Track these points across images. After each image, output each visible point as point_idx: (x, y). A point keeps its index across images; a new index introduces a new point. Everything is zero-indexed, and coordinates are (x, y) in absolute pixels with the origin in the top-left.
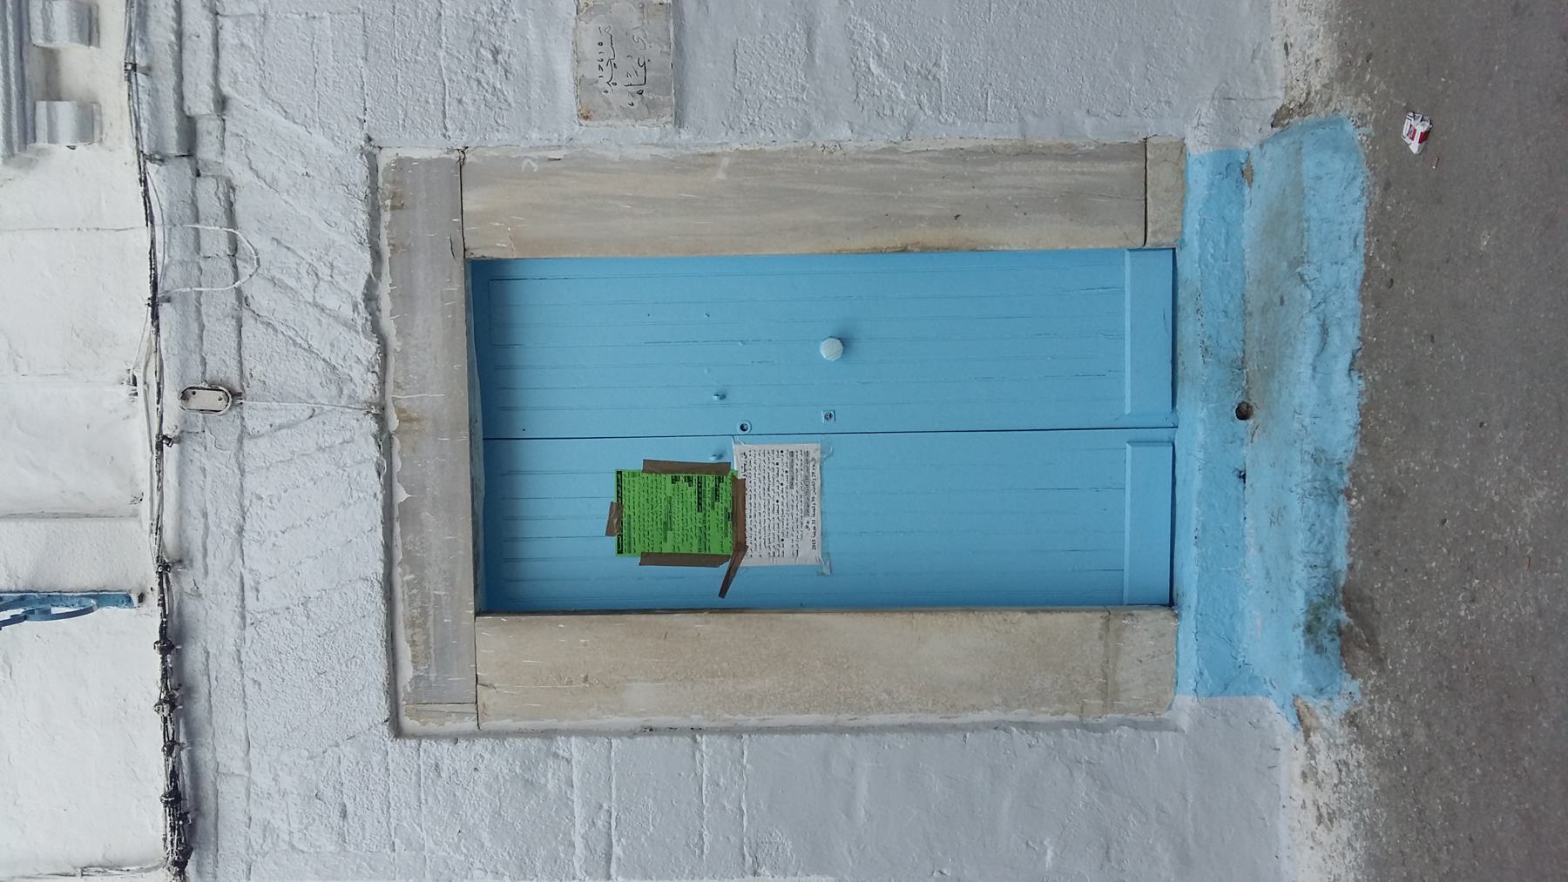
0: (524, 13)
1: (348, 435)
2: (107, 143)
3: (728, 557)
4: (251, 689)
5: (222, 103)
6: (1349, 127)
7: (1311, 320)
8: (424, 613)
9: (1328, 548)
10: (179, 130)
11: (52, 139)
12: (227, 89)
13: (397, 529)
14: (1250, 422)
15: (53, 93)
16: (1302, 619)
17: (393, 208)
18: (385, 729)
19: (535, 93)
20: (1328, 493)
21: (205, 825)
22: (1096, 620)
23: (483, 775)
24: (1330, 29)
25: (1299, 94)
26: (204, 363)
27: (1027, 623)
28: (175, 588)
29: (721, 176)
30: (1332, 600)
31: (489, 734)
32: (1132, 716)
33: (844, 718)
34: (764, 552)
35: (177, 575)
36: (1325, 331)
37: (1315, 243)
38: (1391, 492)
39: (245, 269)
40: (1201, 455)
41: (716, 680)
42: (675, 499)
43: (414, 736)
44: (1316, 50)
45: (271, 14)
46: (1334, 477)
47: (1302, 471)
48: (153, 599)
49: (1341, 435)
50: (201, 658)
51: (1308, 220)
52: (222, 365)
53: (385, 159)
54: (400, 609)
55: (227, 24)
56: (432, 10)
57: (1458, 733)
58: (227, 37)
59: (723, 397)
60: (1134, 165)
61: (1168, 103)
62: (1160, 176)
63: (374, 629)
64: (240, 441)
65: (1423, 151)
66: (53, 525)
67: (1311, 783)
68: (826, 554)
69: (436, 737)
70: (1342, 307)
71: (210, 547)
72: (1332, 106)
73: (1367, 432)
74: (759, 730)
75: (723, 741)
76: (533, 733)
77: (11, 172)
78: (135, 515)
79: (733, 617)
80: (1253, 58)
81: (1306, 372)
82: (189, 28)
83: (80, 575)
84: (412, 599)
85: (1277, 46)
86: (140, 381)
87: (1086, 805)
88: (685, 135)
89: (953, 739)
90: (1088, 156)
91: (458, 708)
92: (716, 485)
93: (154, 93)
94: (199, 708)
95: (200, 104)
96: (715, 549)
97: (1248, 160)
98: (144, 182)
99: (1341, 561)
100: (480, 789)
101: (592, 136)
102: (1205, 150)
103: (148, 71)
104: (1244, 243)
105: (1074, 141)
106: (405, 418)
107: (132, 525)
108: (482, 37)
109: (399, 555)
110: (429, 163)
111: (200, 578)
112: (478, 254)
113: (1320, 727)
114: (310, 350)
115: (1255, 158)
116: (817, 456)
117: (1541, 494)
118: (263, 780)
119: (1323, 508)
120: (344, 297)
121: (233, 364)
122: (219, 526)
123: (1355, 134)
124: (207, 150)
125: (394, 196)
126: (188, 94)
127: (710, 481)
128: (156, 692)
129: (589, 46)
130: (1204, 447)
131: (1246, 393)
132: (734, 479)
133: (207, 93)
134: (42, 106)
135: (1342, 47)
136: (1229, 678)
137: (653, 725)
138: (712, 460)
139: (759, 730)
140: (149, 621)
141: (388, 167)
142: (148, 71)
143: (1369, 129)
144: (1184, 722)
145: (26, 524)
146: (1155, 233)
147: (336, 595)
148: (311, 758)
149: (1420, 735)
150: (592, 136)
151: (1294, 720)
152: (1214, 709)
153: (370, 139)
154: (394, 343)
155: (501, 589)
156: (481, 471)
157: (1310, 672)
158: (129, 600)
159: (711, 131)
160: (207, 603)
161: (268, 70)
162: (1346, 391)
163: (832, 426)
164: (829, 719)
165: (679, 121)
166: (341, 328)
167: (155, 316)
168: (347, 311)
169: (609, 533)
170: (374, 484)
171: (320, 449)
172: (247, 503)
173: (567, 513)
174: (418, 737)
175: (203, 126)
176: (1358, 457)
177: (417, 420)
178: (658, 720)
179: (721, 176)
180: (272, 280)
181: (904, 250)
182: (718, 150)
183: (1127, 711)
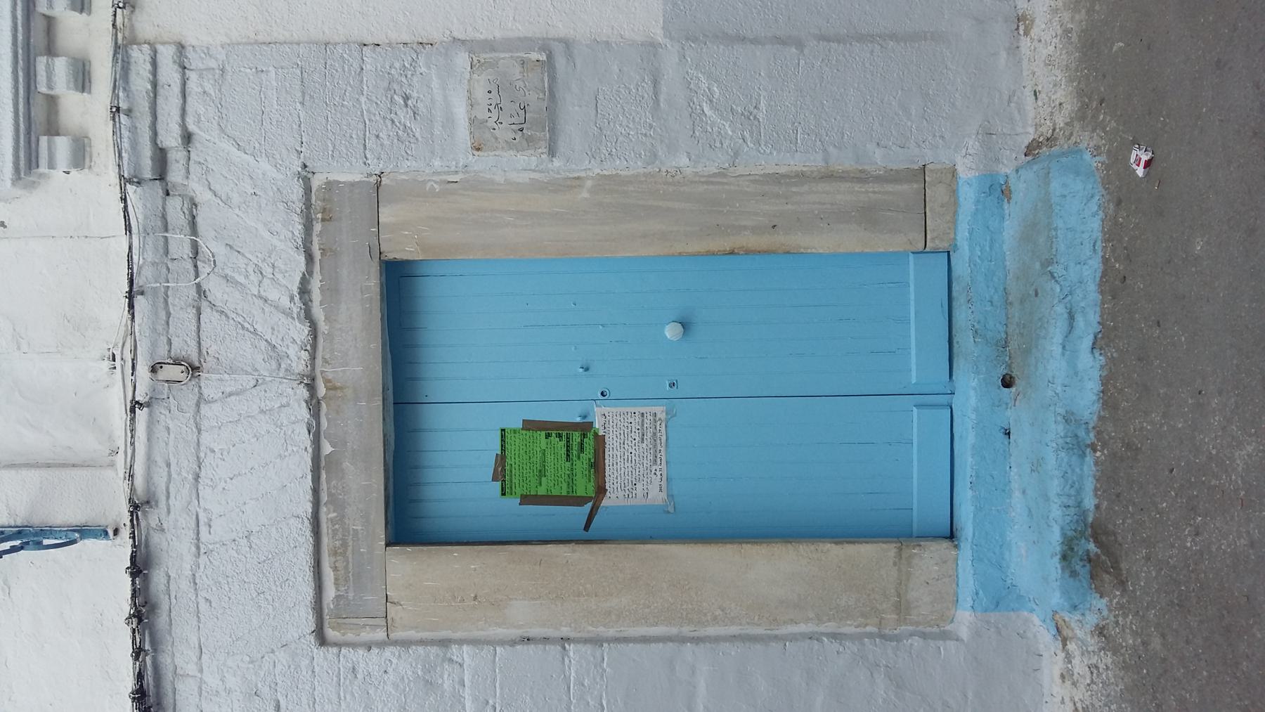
0: (429, 68)
1: (284, 401)
2: (95, 169)
3: (589, 499)
4: (203, 606)
5: (187, 138)
6: (1087, 156)
7: (1060, 309)
8: (344, 545)
9: (1079, 491)
10: (152, 159)
11: (51, 166)
12: (192, 127)
13: (324, 476)
14: (1013, 389)
15: (53, 129)
16: (1058, 549)
17: (323, 220)
18: (312, 638)
19: (437, 131)
20: (1077, 447)
22: (890, 550)
23: (391, 676)
24: (1071, 80)
25: (1046, 130)
26: (170, 343)
27: (835, 552)
28: (143, 524)
29: (585, 195)
30: (1082, 533)
31: (395, 643)
32: (921, 628)
33: (687, 630)
34: (621, 494)
35: (145, 513)
36: (1071, 317)
37: (1062, 248)
38: (1128, 446)
39: (204, 269)
40: (973, 416)
41: (582, 599)
42: (548, 451)
43: (336, 644)
44: (1060, 95)
45: (228, 68)
46: (1082, 433)
47: (1056, 430)
48: (125, 533)
49: (1087, 400)
50: (163, 580)
51: (1056, 229)
52: (184, 345)
53: (317, 182)
54: (325, 540)
55: (193, 76)
56: (356, 66)
57: (1188, 642)
58: (193, 85)
59: (587, 369)
60: (915, 186)
61: (942, 137)
62: (937, 194)
64: (198, 405)
65: (1147, 175)
66: (44, 473)
67: (1068, 683)
68: (671, 496)
69: (353, 645)
70: (1085, 298)
71: (172, 490)
72: (1073, 139)
73: (1108, 398)
74: (617, 640)
75: (587, 649)
76: (432, 642)
77: (18, 192)
78: (112, 465)
79: (595, 547)
80: (1009, 101)
81: (1057, 350)
82: (162, 78)
83: (67, 513)
84: (335, 532)
85: (1028, 93)
86: (118, 358)
87: (884, 700)
88: (557, 163)
89: (775, 646)
90: (878, 179)
91: (371, 621)
92: (582, 440)
93: (133, 130)
94: (162, 620)
95: (170, 139)
96: (580, 492)
97: (1006, 182)
98: (124, 200)
99: (1089, 502)
100: (390, 688)
101: (483, 164)
102: (971, 174)
103: (129, 113)
104: (1005, 247)
105: (867, 167)
106: (331, 387)
107: (109, 473)
108: (395, 86)
109: (324, 497)
110: (352, 185)
111: (163, 517)
112: (391, 256)
113: (1074, 637)
114: (255, 332)
115: (1012, 181)
116: (663, 416)
117: (1250, 449)
118: (212, 680)
119: (1074, 458)
121: (193, 344)
122: (179, 474)
123: (1092, 162)
124: (175, 175)
125: (324, 211)
126: (161, 131)
127: (576, 437)
128: (127, 609)
129: (480, 93)
130: (976, 410)
131: (1009, 366)
132: (596, 435)
133: (176, 130)
134: (44, 140)
135: (1080, 93)
136: (1000, 597)
137: (530, 635)
138: (578, 420)
139: (617, 640)
140: (121, 550)
141: (320, 188)
142: (129, 113)
143: (1103, 158)
144: (964, 633)
145: (24, 473)
146: (933, 239)
147: (274, 530)
148: (252, 662)
149: (1156, 643)
150: (483, 164)
151: (1054, 631)
152: (988, 622)
153: (305, 166)
154: (323, 327)
155: (407, 524)
156: (391, 428)
157: (1065, 593)
158: (106, 533)
159: (577, 160)
160: (169, 536)
161: (224, 111)
162: (1090, 365)
163: (674, 392)
164: (674, 631)
165: (552, 152)
166: (281, 316)
167: (131, 306)
168: (285, 302)
169: (495, 479)
170: (305, 440)
171: (262, 412)
172: (202, 455)
173: (461, 465)
174: (339, 645)
175: (172, 156)
176: (1101, 418)
177: (341, 388)
178: (535, 632)
179: (585, 195)
180: (226, 277)
181: (732, 253)
182: (583, 174)
183: (917, 624)
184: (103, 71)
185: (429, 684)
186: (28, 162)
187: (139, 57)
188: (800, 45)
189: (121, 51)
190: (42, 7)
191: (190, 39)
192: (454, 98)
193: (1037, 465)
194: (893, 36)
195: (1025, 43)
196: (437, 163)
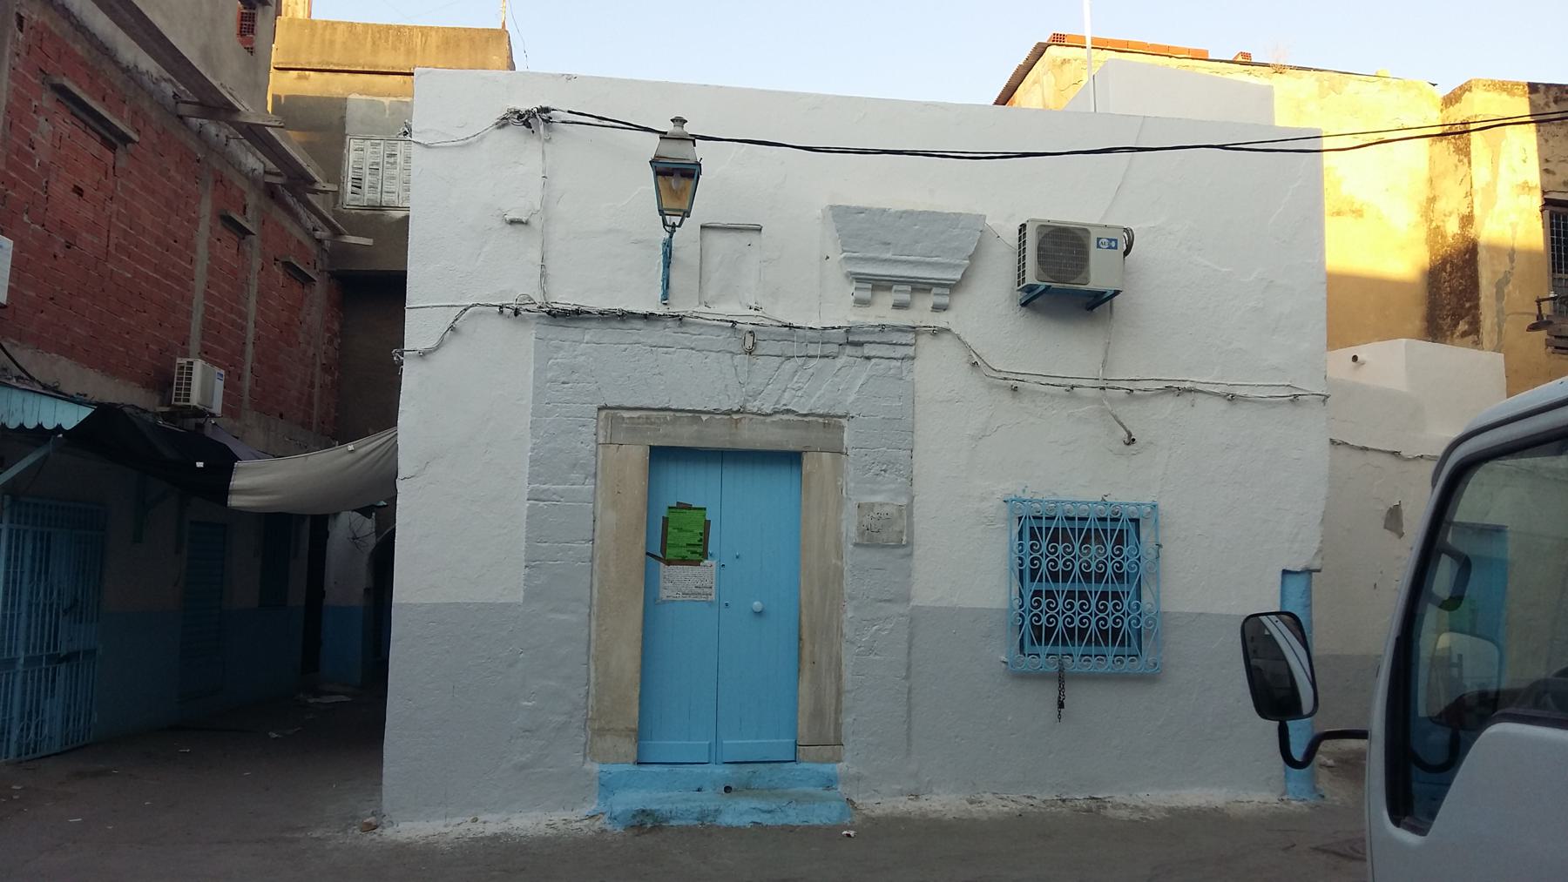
5: (868, 358)
20: (702, 816)
22: (635, 726)
27: (636, 694)
33: (595, 609)
39: (800, 361)
49: (727, 819)
53: (844, 421)
55: (898, 363)
58: (894, 363)
73: (729, 829)
92: (697, 553)
93: (873, 333)
95: (868, 350)
99: (673, 823)
112: (805, 457)
123: (847, 821)
124: (849, 350)
127: (700, 550)
129: (887, 509)
135: (879, 818)
144: (587, 766)
150: (850, 507)
154: (769, 419)
155: (660, 455)
162: (746, 821)
165: (856, 545)
170: (711, 408)
173: (693, 487)
184: (903, 318)
186: (859, 279)
187: (909, 338)
188: (907, 678)
189: (913, 329)
190: (935, 290)
191: (916, 362)
192: (883, 497)
193: (687, 800)
194: (909, 728)
195: (904, 798)
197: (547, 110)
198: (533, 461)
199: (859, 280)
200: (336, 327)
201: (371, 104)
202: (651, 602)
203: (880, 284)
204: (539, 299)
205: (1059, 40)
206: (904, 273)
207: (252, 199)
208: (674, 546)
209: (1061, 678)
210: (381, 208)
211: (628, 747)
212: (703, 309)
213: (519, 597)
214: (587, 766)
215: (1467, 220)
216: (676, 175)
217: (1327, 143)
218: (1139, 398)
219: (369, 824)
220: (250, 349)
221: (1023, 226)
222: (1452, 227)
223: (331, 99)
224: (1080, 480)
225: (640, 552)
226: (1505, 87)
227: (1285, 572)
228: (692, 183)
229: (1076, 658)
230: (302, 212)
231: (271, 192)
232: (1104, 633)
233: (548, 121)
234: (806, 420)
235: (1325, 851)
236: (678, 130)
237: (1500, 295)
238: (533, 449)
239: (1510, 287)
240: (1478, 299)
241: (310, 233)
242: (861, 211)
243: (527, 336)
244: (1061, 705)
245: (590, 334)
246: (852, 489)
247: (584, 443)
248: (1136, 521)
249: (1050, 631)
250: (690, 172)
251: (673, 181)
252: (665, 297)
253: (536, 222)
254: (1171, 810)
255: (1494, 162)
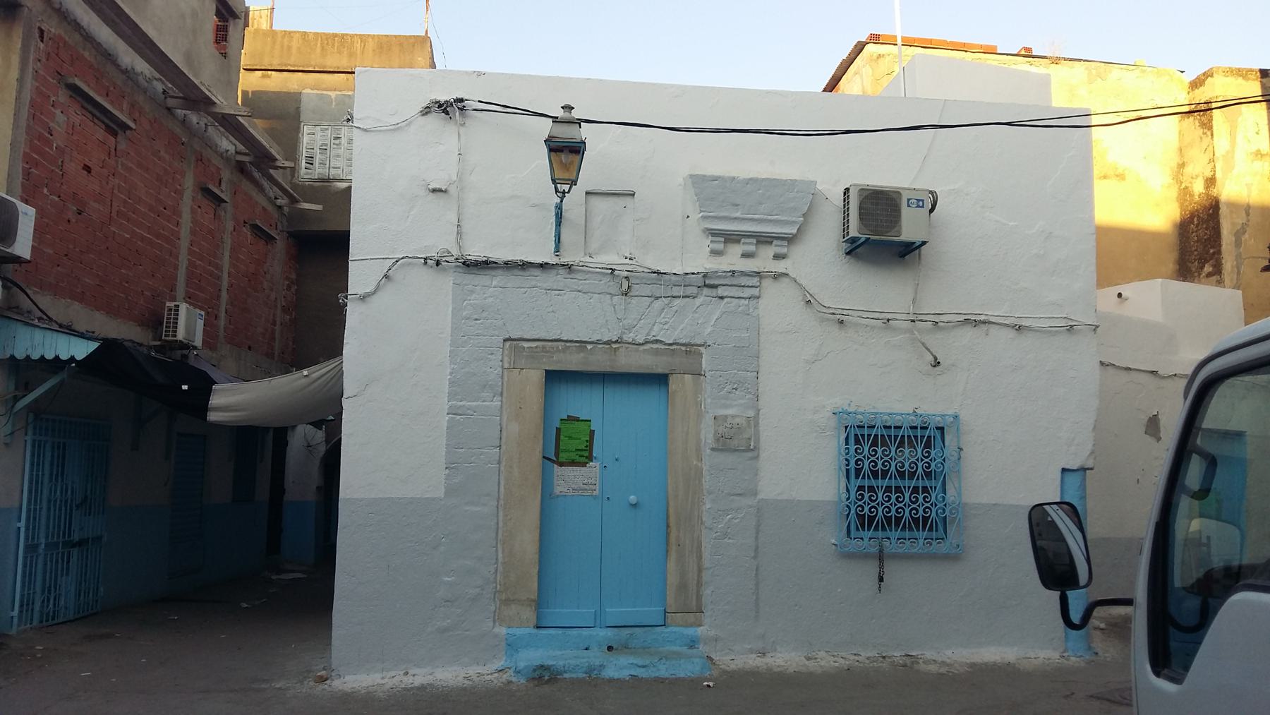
5: (722, 298)
7: (647, 662)
20: (590, 670)
21: (474, 270)
22: (534, 596)
27: (535, 571)
33: (502, 502)
39: (666, 301)
49: (610, 673)
52: (636, 290)
58: (743, 301)
62: (691, 617)
63: (543, 335)
73: (611, 681)
90: (698, 592)
92: (584, 457)
93: (725, 277)
94: (516, 272)
95: (721, 291)
96: (561, 455)
99: (566, 676)
112: (672, 379)
120: (658, 332)
123: (707, 674)
124: (706, 291)
127: (586, 454)
129: (737, 420)
136: (512, 646)
140: (552, 260)
144: (497, 630)
150: (708, 421)
154: (642, 348)
155: (554, 378)
157: (526, 667)
162: (625, 674)
165: (713, 449)
170: (594, 339)
178: (504, 433)
185: (485, 386)
186: (714, 233)
187: (755, 281)
188: (755, 557)
189: (758, 274)
190: (775, 242)
191: (761, 301)
192: (735, 410)
194: (757, 599)
195: (754, 656)
196: (709, 400)
197: (461, 100)
198: (452, 383)
199: (713, 235)
200: (293, 276)
201: (321, 97)
202: (547, 496)
203: (731, 238)
204: (455, 252)
205: (875, 39)
206: (750, 229)
207: (226, 175)
208: (566, 451)
209: (881, 557)
210: (328, 180)
211: (529, 614)
212: (588, 259)
213: (441, 493)
214: (497, 630)
215: (1210, 182)
216: (566, 151)
217: (1095, 120)
218: (942, 329)
219: (321, 677)
220: (224, 294)
221: (847, 189)
222: (1198, 188)
223: (288, 94)
224: (895, 395)
225: (538, 455)
226: (1241, 73)
227: (1064, 470)
228: (578, 158)
229: (893, 541)
230: (265, 183)
231: (241, 168)
232: (916, 521)
233: (462, 109)
234: (673, 348)
235: (1098, 698)
236: (567, 115)
237: (1238, 243)
238: (451, 374)
239: (1247, 236)
240: (1220, 246)
241: (272, 202)
242: (715, 179)
243: (446, 283)
244: (881, 579)
245: (497, 280)
246: (710, 403)
247: (493, 368)
248: (941, 429)
249: (871, 519)
250: (577, 149)
251: (563, 156)
252: (557, 250)
253: (453, 190)
254: (973, 665)
255: (1233, 135)
